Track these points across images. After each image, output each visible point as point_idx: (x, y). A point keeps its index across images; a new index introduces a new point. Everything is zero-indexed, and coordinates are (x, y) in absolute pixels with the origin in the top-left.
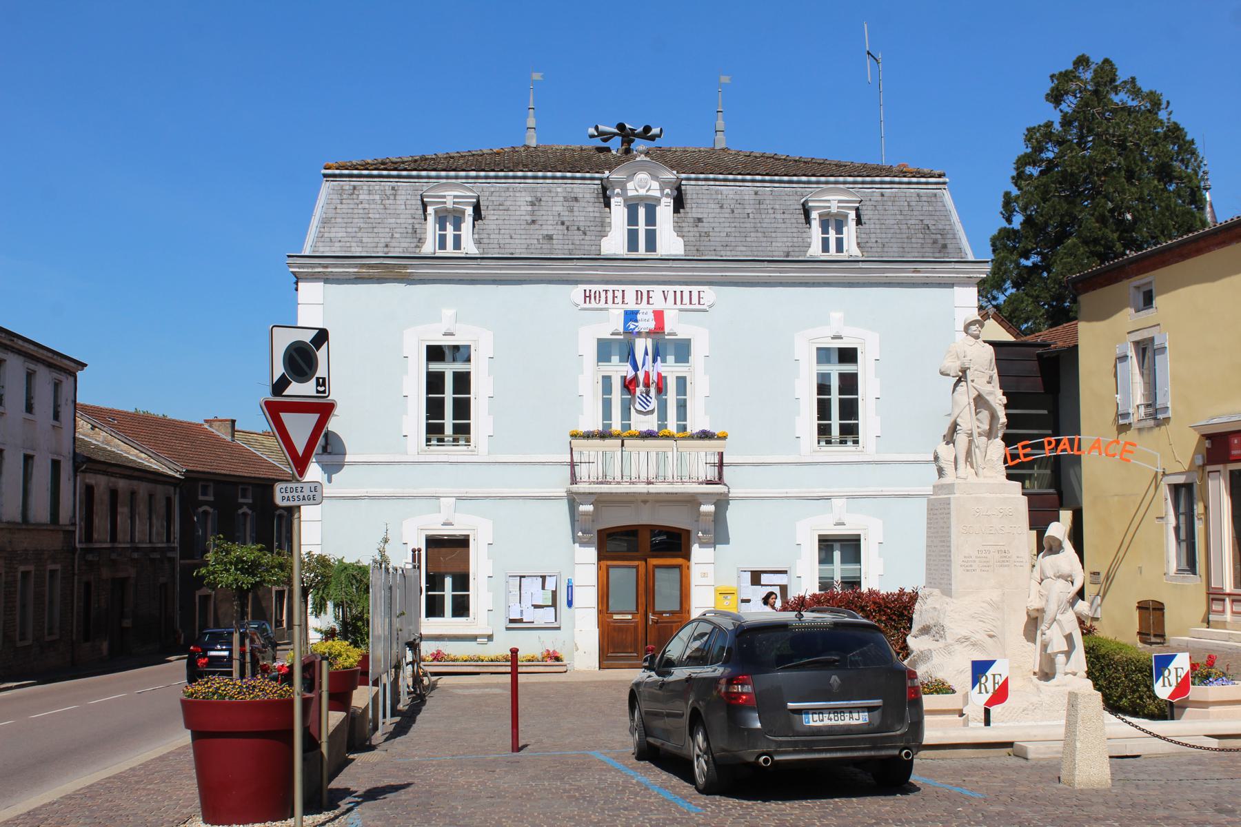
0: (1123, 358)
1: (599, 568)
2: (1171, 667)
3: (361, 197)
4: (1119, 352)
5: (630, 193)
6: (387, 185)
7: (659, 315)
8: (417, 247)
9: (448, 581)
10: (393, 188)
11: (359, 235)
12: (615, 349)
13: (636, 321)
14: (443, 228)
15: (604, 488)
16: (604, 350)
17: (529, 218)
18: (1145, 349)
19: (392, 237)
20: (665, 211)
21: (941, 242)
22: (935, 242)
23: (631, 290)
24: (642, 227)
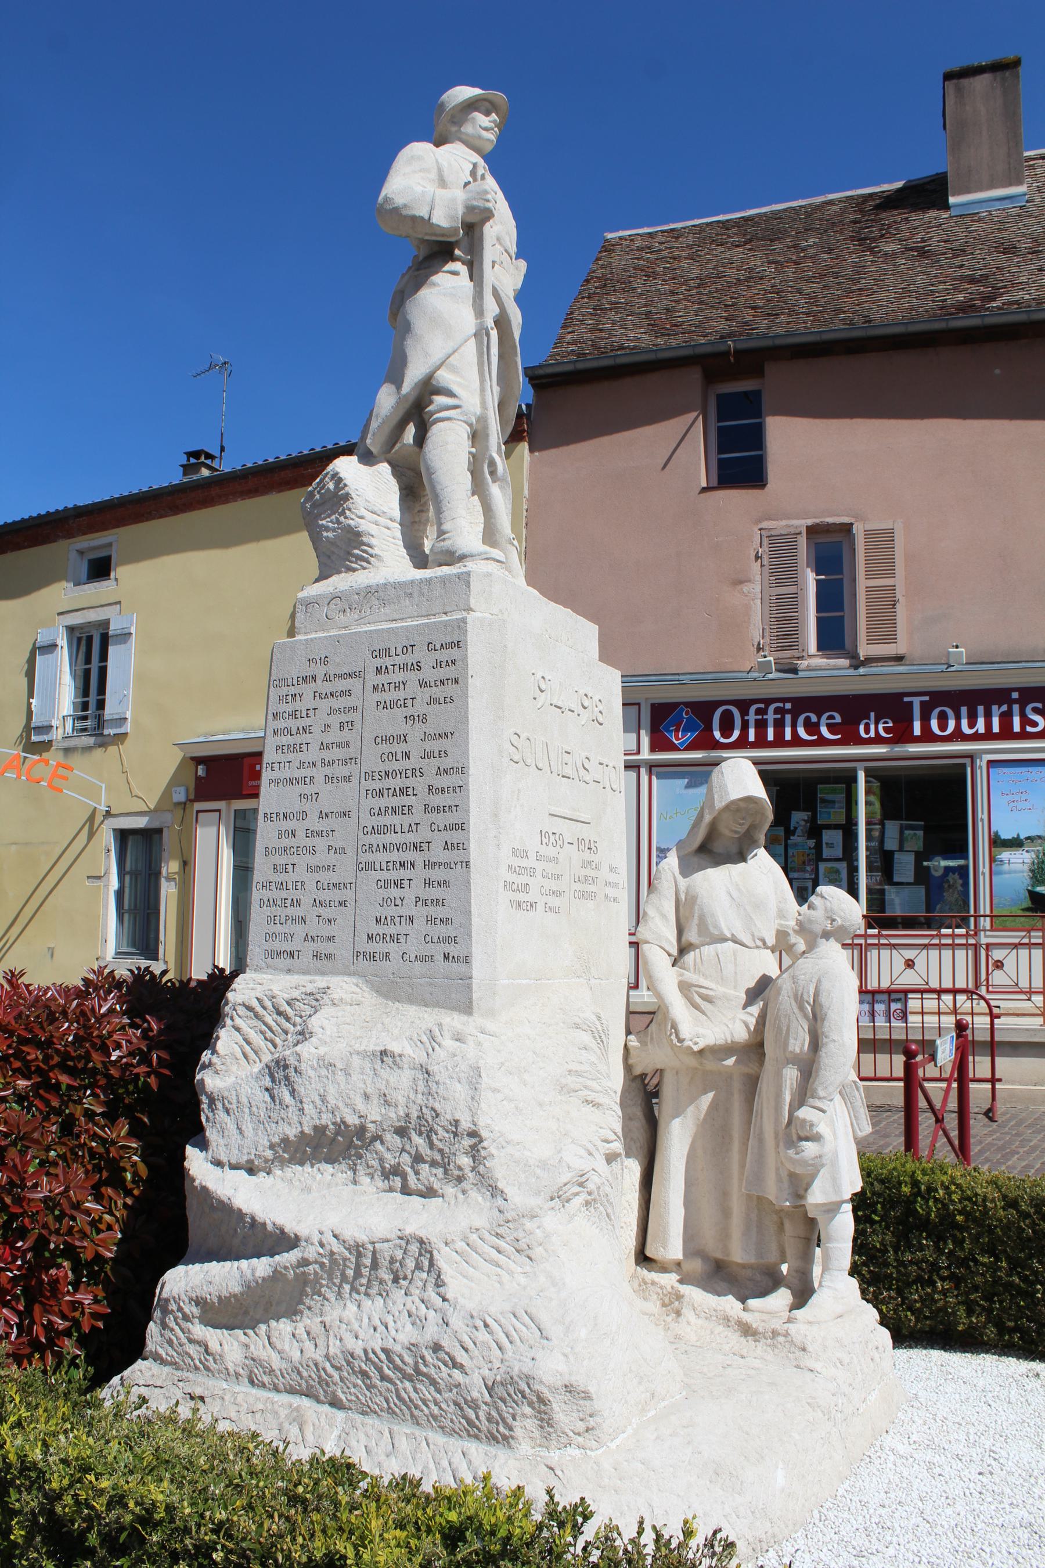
0: (51, 648)
4: (42, 639)
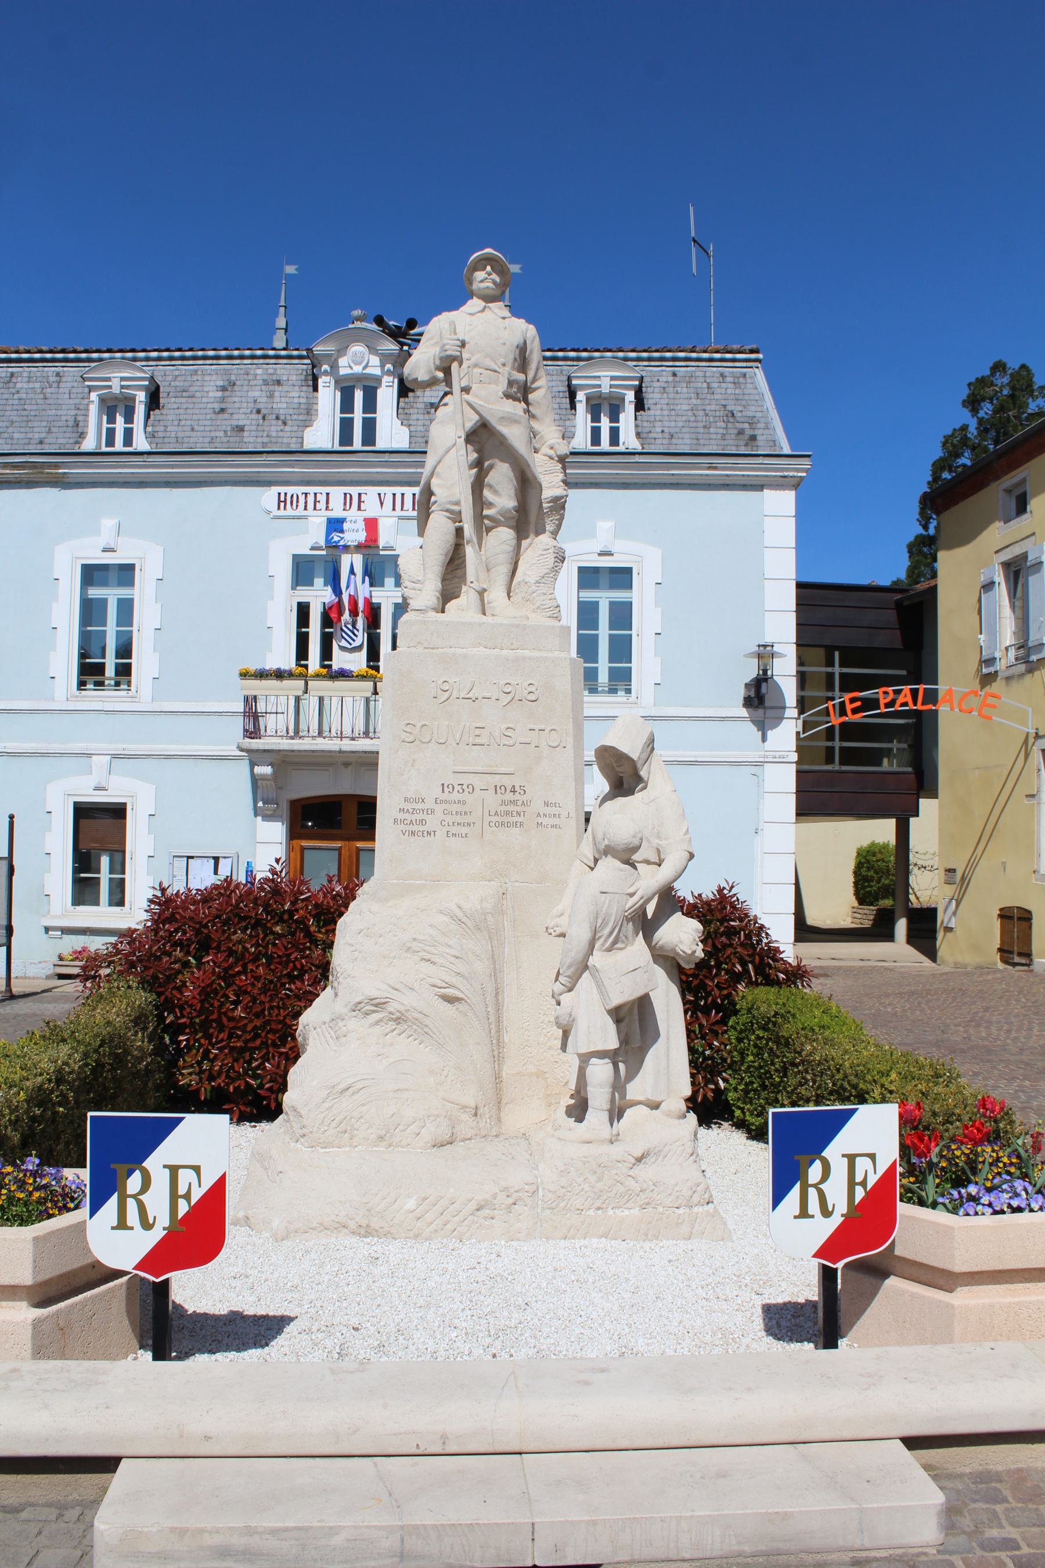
0: (989, 586)
1: (290, 849)
2: (834, 1152)
3: (19, 385)
5: (343, 371)
6: (50, 370)
7: (371, 525)
8: (77, 443)
9: (105, 861)
10: (58, 374)
11: (11, 430)
12: (319, 568)
13: (342, 531)
14: (112, 420)
15: (297, 744)
16: (303, 570)
17: (217, 406)
18: (1017, 571)
19: (49, 432)
20: (387, 395)
21: (749, 432)
22: (741, 432)
23: (337, 493)
24: (358, 415)
